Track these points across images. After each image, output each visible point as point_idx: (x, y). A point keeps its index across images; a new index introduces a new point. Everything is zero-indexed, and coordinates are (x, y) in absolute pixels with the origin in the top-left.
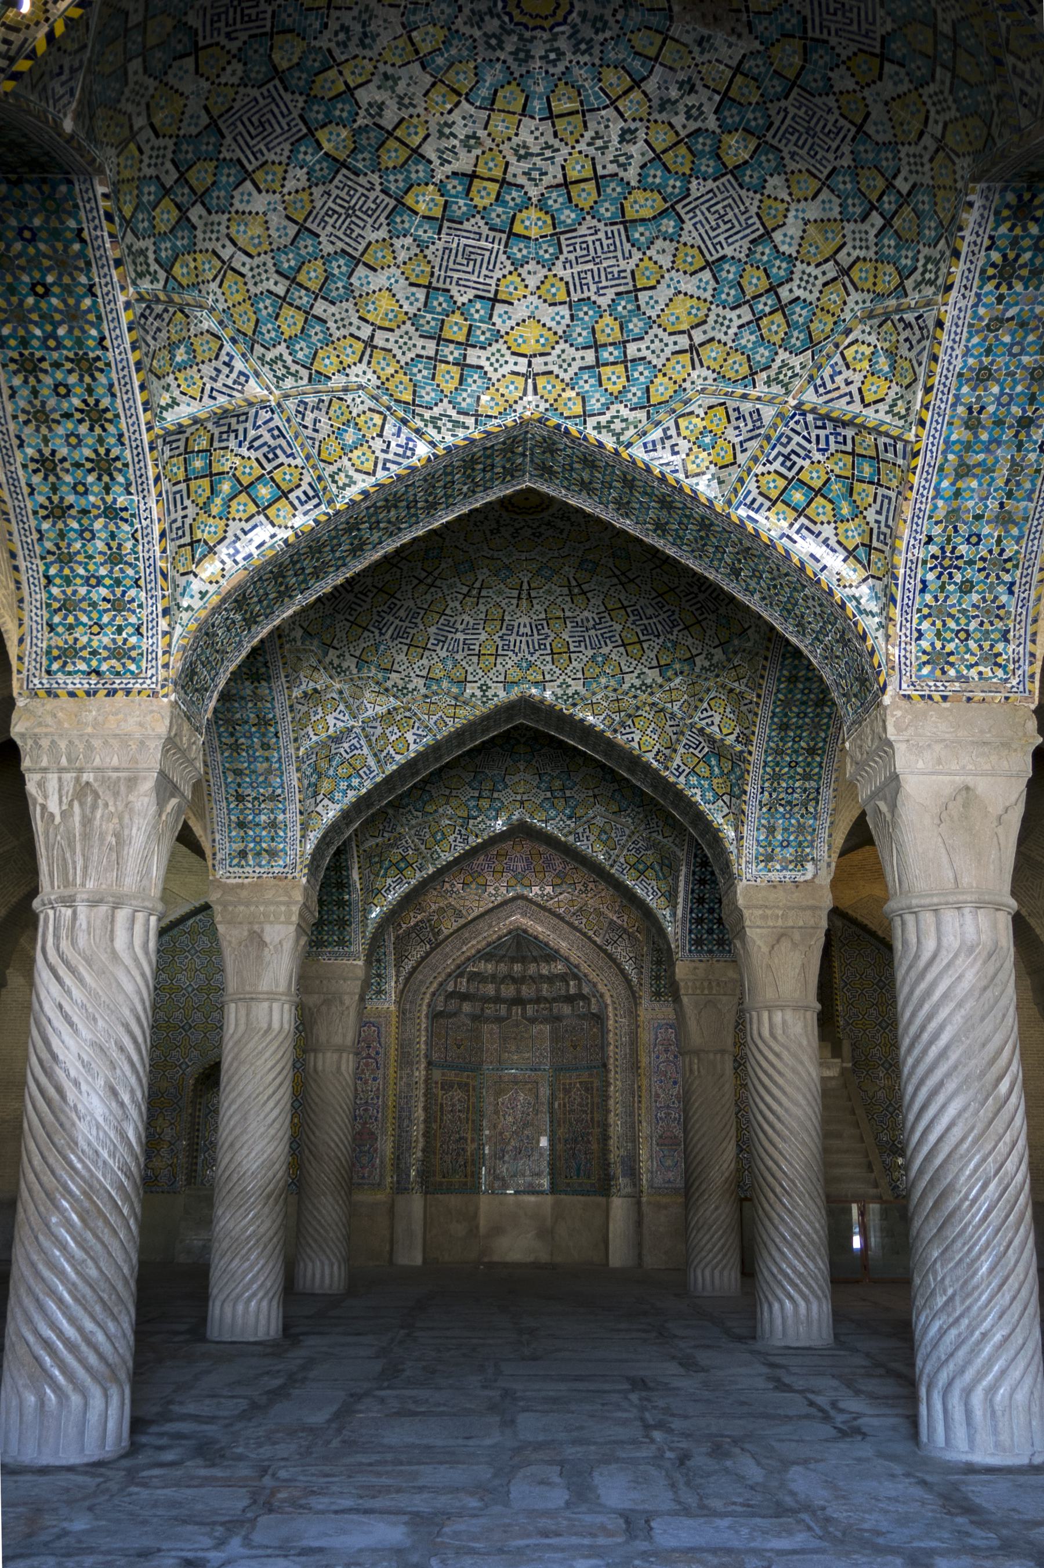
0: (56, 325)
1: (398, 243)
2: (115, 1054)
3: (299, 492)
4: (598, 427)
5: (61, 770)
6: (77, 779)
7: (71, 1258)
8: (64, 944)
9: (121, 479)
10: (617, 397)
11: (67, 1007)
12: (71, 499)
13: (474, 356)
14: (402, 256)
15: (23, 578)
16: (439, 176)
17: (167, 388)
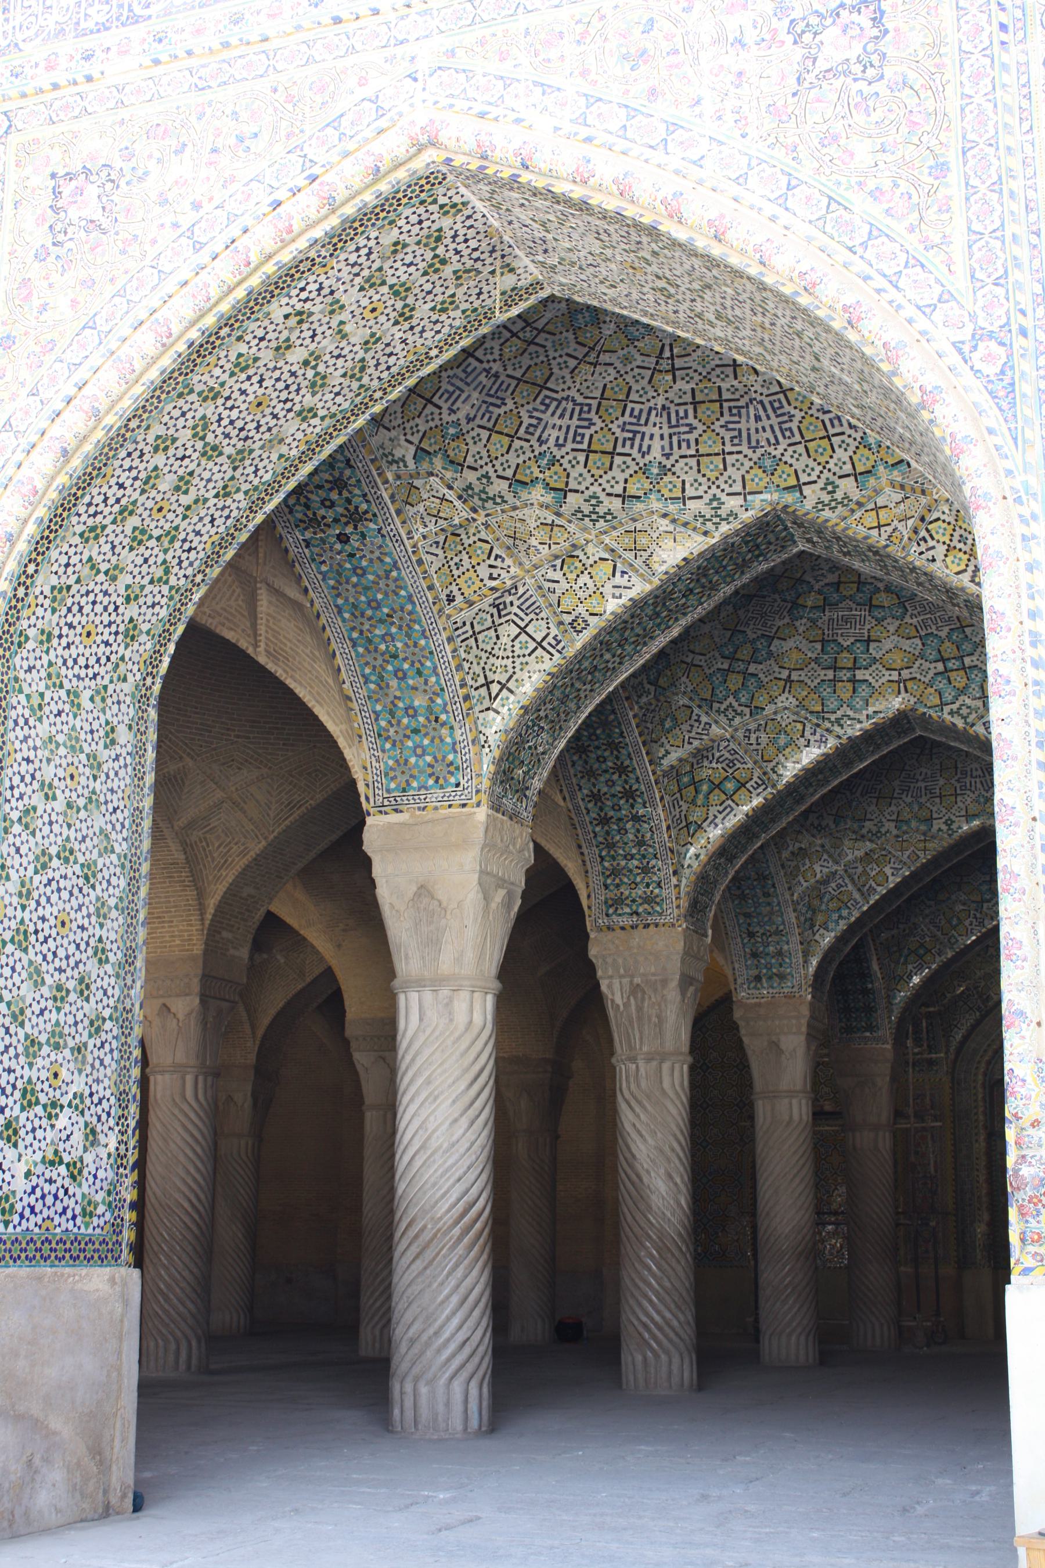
0: (595, 729)
1: (797, 624)
2: (669, 1153)
3: (752, 783)
4: (951, 713)
5: (621, 977)
6: (631, 982)
7: (654, 1276)
8: (633, 1086)
9: (640, 800)
10: (963, 691)
11: (638, 1125)
12: (611, 813)
13: (860, 675)
14: (801, 629)
15: (587, 859)
16: (816, 588)
17: (662, 745)
